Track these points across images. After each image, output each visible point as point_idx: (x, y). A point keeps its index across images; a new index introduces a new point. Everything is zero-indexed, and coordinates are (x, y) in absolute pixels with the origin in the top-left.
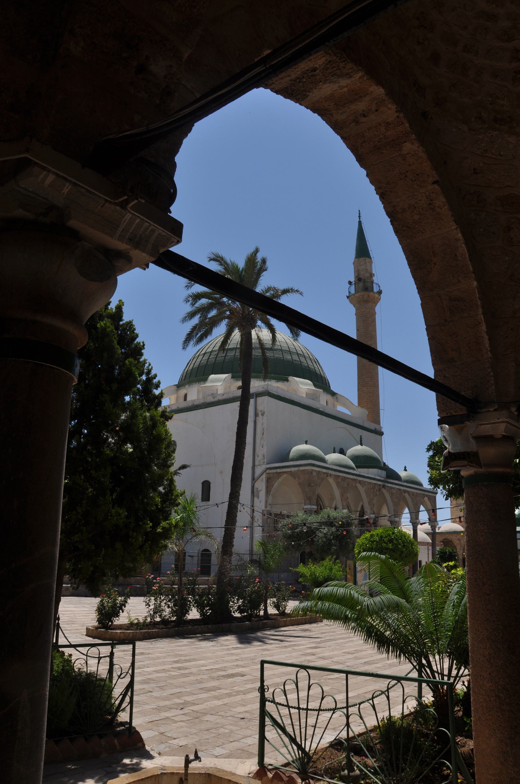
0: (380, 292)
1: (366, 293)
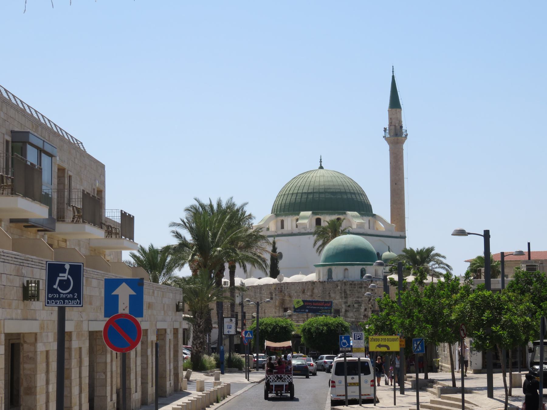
0: (406, 135)
1: (396, 138)
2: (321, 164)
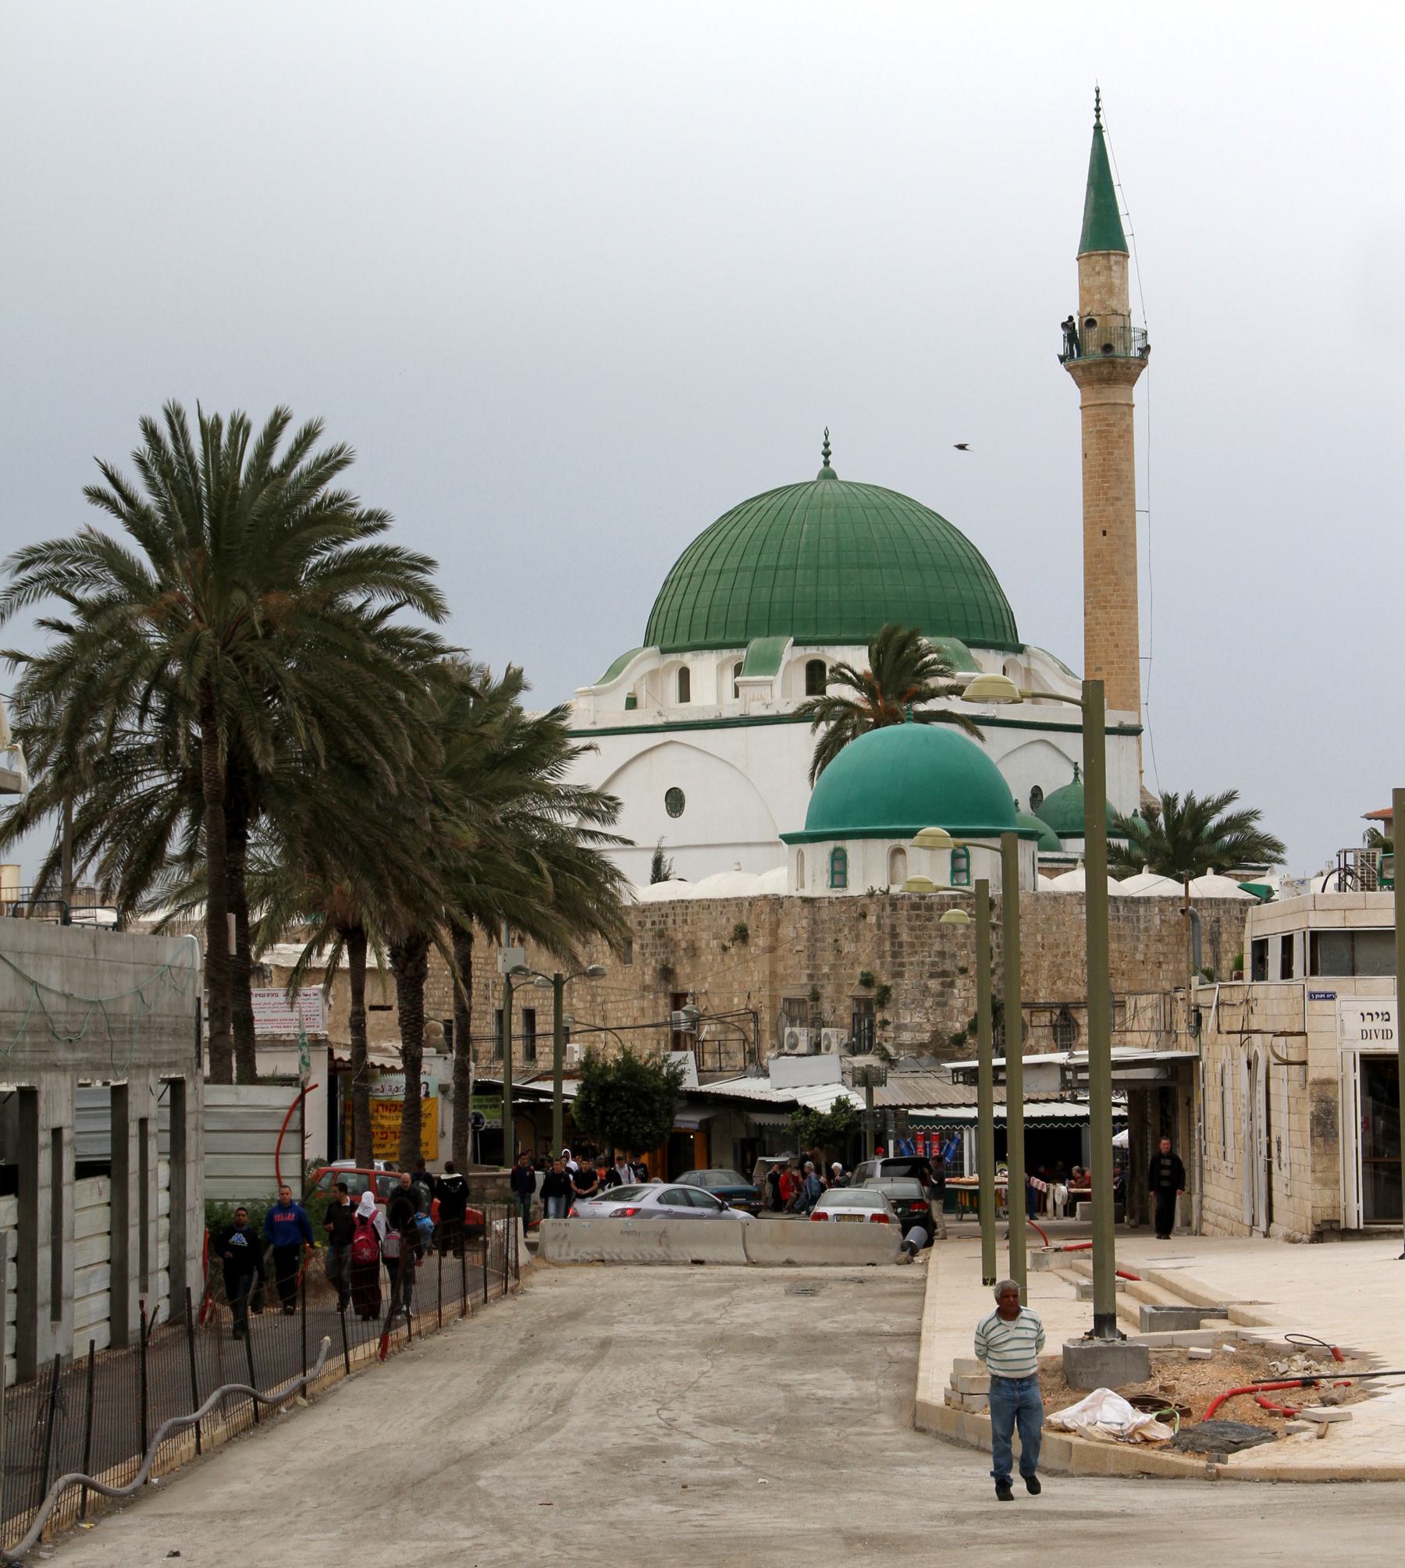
2: (827, 463)
